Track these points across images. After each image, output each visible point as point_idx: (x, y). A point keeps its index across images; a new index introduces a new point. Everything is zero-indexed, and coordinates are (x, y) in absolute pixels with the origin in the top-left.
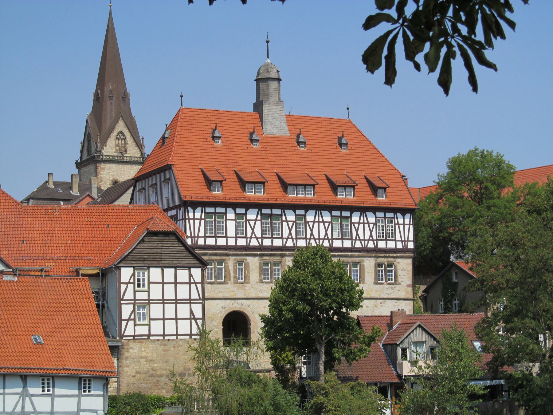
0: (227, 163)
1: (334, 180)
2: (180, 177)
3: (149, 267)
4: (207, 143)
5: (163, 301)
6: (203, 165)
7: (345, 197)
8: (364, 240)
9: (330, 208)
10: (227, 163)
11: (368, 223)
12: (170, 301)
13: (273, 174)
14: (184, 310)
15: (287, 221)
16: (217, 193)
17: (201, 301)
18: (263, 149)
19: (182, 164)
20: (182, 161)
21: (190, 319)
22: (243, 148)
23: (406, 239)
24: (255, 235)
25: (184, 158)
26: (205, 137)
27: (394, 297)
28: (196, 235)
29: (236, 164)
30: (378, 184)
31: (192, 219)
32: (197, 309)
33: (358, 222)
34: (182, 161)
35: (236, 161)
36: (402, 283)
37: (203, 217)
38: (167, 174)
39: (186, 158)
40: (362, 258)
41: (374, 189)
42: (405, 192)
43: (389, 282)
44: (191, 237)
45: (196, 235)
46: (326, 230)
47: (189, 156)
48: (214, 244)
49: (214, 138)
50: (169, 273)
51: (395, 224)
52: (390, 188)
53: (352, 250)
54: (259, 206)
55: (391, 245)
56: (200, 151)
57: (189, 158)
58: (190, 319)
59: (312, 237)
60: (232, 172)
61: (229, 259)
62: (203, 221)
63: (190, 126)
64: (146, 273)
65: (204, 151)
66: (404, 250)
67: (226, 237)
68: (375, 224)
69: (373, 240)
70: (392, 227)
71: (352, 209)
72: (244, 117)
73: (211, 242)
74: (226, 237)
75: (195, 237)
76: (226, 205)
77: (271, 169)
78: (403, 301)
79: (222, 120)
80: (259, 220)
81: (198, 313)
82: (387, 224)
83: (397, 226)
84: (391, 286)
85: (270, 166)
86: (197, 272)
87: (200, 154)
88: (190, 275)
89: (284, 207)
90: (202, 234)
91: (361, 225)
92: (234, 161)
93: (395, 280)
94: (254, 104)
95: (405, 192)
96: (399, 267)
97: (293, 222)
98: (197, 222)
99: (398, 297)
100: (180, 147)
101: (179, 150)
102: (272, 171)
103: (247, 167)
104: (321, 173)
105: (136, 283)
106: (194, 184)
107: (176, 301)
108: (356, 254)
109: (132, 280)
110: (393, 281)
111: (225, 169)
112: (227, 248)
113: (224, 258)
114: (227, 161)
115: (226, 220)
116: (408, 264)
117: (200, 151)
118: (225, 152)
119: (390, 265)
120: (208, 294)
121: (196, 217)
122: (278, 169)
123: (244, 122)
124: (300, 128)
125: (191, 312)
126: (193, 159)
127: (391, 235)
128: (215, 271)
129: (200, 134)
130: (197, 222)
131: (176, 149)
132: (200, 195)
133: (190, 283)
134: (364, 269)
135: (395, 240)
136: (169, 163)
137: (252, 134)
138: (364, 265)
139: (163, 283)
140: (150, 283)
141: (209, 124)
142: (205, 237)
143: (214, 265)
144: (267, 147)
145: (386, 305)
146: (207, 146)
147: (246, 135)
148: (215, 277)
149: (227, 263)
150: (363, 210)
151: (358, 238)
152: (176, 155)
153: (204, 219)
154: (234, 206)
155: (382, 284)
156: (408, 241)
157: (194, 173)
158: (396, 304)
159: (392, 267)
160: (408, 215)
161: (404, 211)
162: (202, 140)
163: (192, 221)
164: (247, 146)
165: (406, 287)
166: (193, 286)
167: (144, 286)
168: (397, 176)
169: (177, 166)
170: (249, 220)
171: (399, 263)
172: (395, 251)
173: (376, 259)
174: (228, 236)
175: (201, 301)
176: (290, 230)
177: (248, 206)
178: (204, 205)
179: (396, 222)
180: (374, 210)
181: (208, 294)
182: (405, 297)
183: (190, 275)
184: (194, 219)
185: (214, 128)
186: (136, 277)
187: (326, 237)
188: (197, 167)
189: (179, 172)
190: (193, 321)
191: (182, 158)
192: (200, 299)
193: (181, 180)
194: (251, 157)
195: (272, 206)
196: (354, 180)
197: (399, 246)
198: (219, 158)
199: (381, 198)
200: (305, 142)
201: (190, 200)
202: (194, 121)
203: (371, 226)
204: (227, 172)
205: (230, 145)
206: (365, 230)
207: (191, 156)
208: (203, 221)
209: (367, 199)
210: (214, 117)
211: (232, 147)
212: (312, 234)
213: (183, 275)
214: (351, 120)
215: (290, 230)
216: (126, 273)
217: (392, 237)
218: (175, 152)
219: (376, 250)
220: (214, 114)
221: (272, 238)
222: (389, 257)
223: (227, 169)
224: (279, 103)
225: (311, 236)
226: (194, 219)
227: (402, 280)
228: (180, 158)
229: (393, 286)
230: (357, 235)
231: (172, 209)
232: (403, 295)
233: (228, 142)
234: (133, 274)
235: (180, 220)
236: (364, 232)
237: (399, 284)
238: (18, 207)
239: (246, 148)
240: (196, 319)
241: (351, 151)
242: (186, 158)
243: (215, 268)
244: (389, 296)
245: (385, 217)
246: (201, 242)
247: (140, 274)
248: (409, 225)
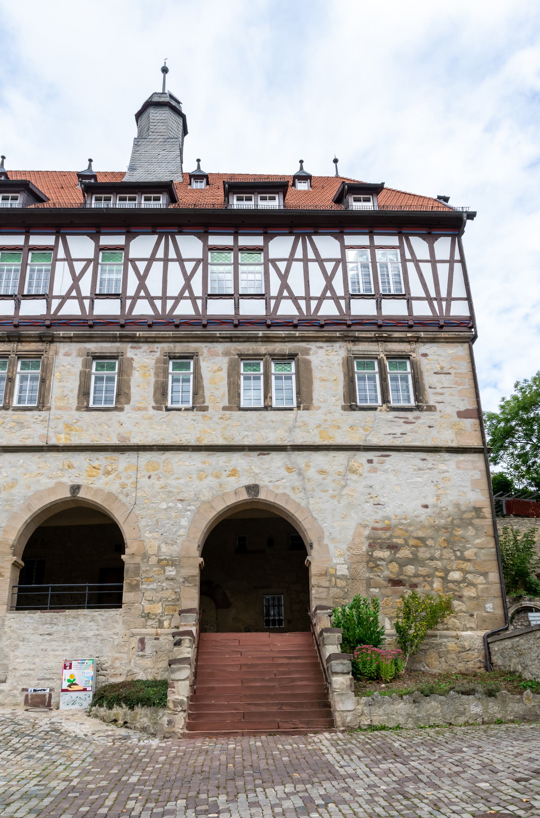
23: (444, 294)
33: (287, 256)
36: (439, 407)
40: (304, 345)
53: (269, 323)
78: (446, 456)
83: (411, 266)
93: (417, 399)
96: (426, 366)
99: (429, 443)
108: (282, 333)
134: (309, 371)
138: (308, 363)
145: (386, 466)
155: (374, 409)
158: (421, 464)
165: (456, 418)
173: (350, 346)
203: (329, 267)
227: (439, 398)
229: (410, 415)
232: (448, 438)
237: (430, 409)
244: (398, 442)
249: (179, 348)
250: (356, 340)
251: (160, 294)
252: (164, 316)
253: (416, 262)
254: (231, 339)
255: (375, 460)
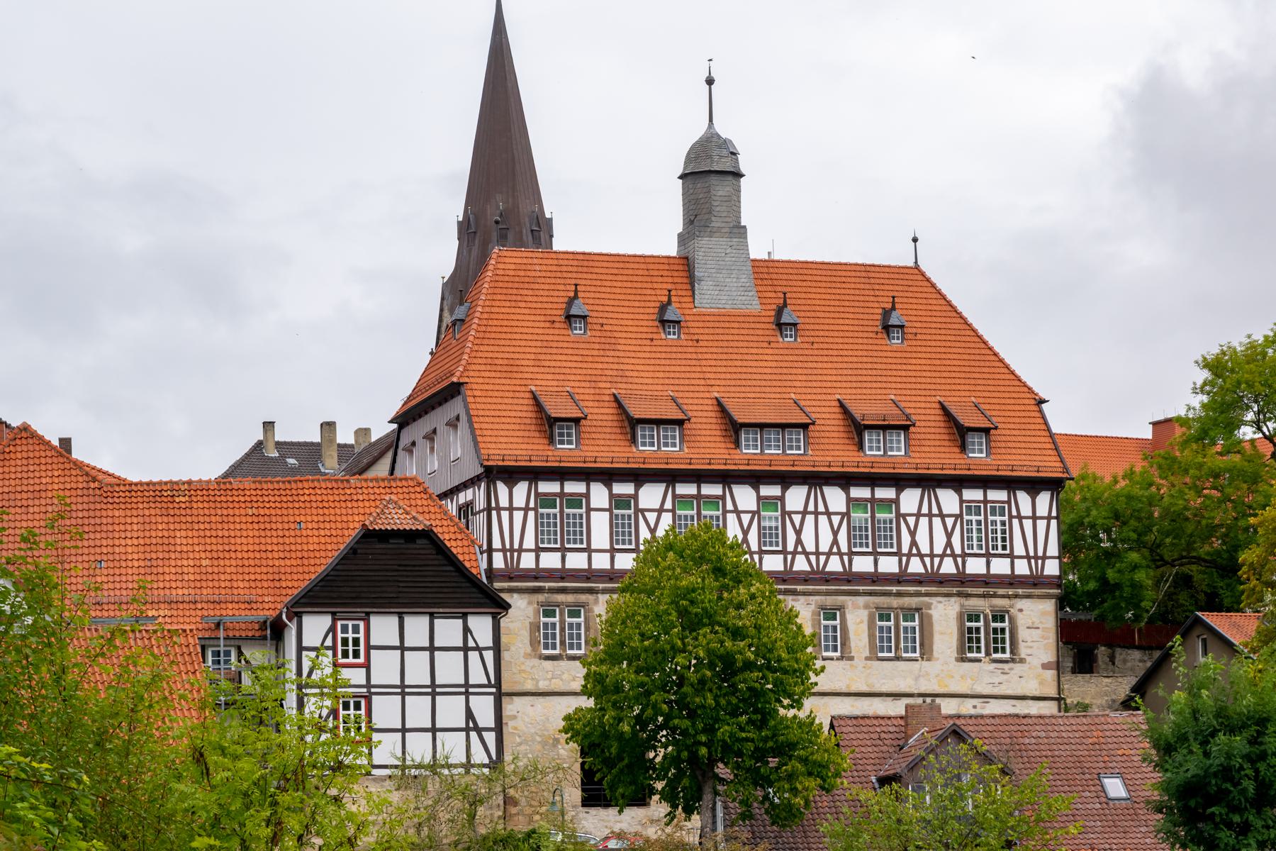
0: (599, 378)
1: (857, 410)
2: (481, 413)
3: (368, 614)
4: (551, 331)
5: (403, 690)
6: (538, 383)
7: (882, 452)
8: (932, 556)
9: (845, 480)
10: (599, 378)
11: (942, 516)
12: (418, 691)
13: (710, 402)
14: (451, 710)
15: (737, 512)
16: (566, 451)
17: (494, 690)
18: (690, 343)
19: (487, 380)
20: (487, 374)
21: (467, 730)
22: (639, 342)
24: (838, 548)
25: (494, 368)
26: (549, 318)
27: (1010, 692)
28: (516, 546)
29: (619, 379)
30: (968, 420)
31: (505, 509)
32: (484, 708)
34: (487, 374)
35: (620, 373)
36: (1028, 659)
37: (532, 505)
38: (454, 407)
39: (499, 368)
40: (926, 599)
41: (960, 434)
42: (1043, 439)
43: (995, 656)
44: (504, 550)
45: (516, 546)
46: (835, 533)
47: (506, 362)
48: (609, 567)
49: (569, 318)
50: (417, 628)
51: (1011, 517)
52: (998, 432)
53: (900, 578)
54: (670, 477)
55: (1000, 567)
56: (534, 350)
57: (505, 368)
58: (467, 730)
59: (800, 549)
60: (607, 398)
61: (596, 602)
62: (531, 514)
63: (515, 291)
64: (362, 624)
65: (544, 350)
66: (1035, 582)
67: (589, 550)
68: (958, 517)
69: (954, 556)
70: (1003, 523)
71: (900, 482)
72: (651, 266)
73: (550, 561)
74: (589, 550)
75: (512, 550)
76: (588, 475)
77: (706, 389)
78: (1031, 702)
79: (594, 276)
80: (667, 511)
81: (485, 717)
82: (990, 518)
83: (1015, 522)
84: (1000, 665)
85: (702, 382)
86: (481, 627)
87: (533, 357)
88: (467, 630)
89: (728, 478)
90: (529, 542)
91: (924, 521)
92: (615, 373)
93: (1012, 652)
94: (680, 235)
95: (1043, 439)
96: (1022, 621)
97: (753, 513)
98: (518, 516)
99: (1019, 692)
100: (485, 342)
101: (482, 348)
102: (707, 395)
103: (645, 387)
104: (829, 397)
105: (362, 648)
106: (513, 427)
107: (434, 690)
108: (911, 589)
109: (329, 642)
110: (1007, 655)
111: (592, 391)
112: (590, 575)
113: (583, 598)
114: (600, 372)
115: (589, 510)
116: (1044, 613)
117: (534, 350)
118: (595, 353)
119: (999, 617)
120: (546, 683)
121: (515, 505)
122: (722, 389)
123: (649, 279)
124: (785, 289)
125: (469, 715)
126: (515, 369)
127: (975, 543)
128: (562, 630)
129: (539, 312)
130: (518, 516)
131: (476, 348)
132: (524, 453)
133: (465, 649)
134: (931, 624)
135: (1012, 556)
136: (455, 379)
137: (663, 308)
138: (930, 617)
139: (402, 648)
140: (369, 647)
141: (562, 287)
142: (538, 550)
143: (562, 614)
144: (701, 337)
146: (551, 338)
147: (652, 311)
148: (563, 643)
149: (591, 611)
150: (928, 482)
151: (914, 551)
152: (475, 361)
153: (535, 509)
154: (608, 476)
155: (979, 660)
156: (1044, 558)
157: (516, 401)
159: (1003, 621)
160: (1044, 499)
161: (1033, 485)
162: (542, 325)
163: (505, 515)
164: (650, 336)
165: (1040, 670)
166: (474, 656)
167: (356, 654)
168: (1027, 402)
169: (474, 386)
170: (643, 511)
171: (1021, 610)
172: (1012, 581)
173: (963, 600)
174: (593, 547)
175: (494, 690)
176: (949, 535)
177: (640, 477)
178: (534, 474)
179: (1014, 513)
180: (958, 483)
181: (546, 683)
182: (1037, 694)
183: (467, 630)
184: (511, 509)
185: (572, 294)
186: (340, 635)
187: (835, 550)
188: (523, 389)
189: (478, 400)
190: (473, 735)
191: (489, 368)
192: (489, 685)
193: (482, 419)
194: (658, 362)
195: (699, 477)
196: (908, 411)
197: (1022, 568)
198: (580, 365)
199: (978, 457)
200: (795, 325)
201: (500, 463)
202: (527, 280)
204: (597, 398)
205: (609, 334)
206: (931, 529)
207: (512, 362)
208: (531, 514)
209: (942, 458)
210: (575, 269)
211: (613, 341)
212: (914, 543)
213: (449, 631)
214: (923, 267)
215: (949, 535)
216: (315, 627)
217: (1004, 548)
218: (474, 354)
219: (962, 582)
220: (575, 263)
221: (875, 554)
222: (995, 596)
223: (597, 391)
224: (736, 230)
225: (796, 547)
226: (511, 509)
227: (1029, 651)
228: (483, 367)
229: (1006, 666)
230: (914, 543)
231: (464, 486)
232: (1032, 688)
233: (605, 327)
234: (332, 629)
235: (480, 512)
236: (931, 537)
237: (1022, 661)
238: (92, 485)
239: (648, 342)
240: (479, 731)
241: (914, 343)
242: (499, 368)
243: (562, 622)
244: (996, 691)
245: (985, 501)
246: (527, 561)
247: (350, 629)
248: (1049, 518)
249: (830, 601)
250: (968, 596)
251: (814, 550)
252: (818, 572)
253: (1020, 518)
254: (871, 594)
255: (979, 705)
